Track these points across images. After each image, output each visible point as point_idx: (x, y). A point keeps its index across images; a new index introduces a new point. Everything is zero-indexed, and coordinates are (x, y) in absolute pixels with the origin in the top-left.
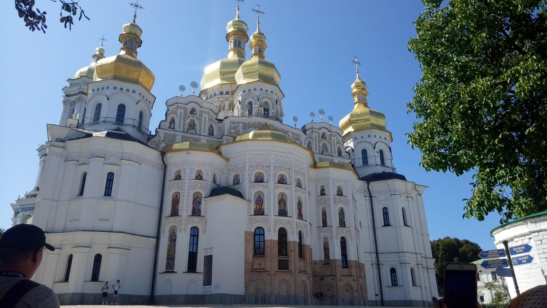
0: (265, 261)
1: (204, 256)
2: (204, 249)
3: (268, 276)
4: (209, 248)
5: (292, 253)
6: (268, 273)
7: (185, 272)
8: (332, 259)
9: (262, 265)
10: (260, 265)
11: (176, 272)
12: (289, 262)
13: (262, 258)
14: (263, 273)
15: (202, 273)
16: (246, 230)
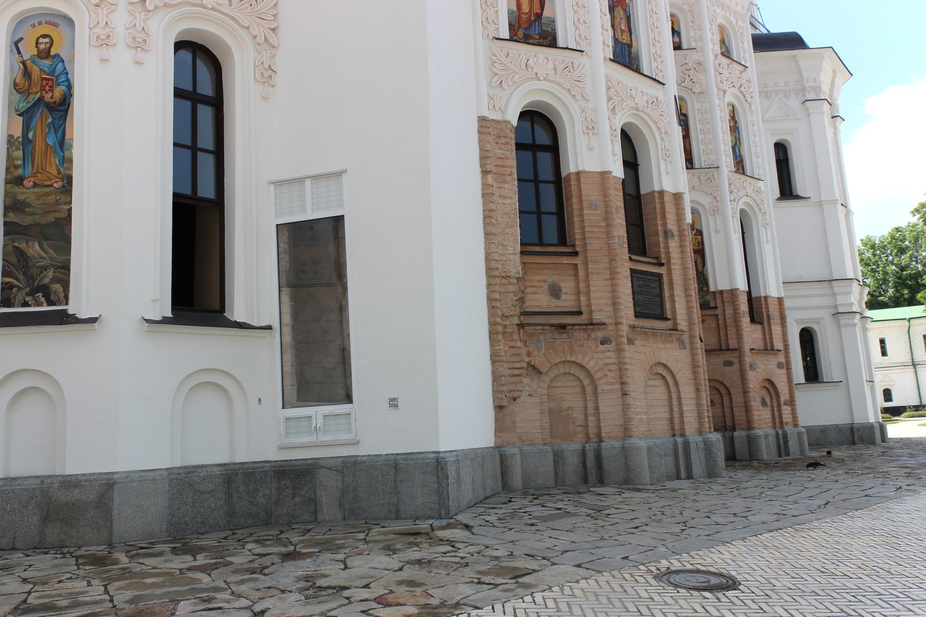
0: (581, 273)
1: (277, 225)
2: (278, 184)
3: (602, 347)
4: (315, 178)
5: (673, 244)
6: (600, 335)
7: (159, 318)
8: (720, 287)
9: (564, 297)
10: (555, 292)
11: (93, 320)
12: (666, 287)
13: (565, 260)
14: (579, 334)
15: (269, 328)
16: (486, 113)
